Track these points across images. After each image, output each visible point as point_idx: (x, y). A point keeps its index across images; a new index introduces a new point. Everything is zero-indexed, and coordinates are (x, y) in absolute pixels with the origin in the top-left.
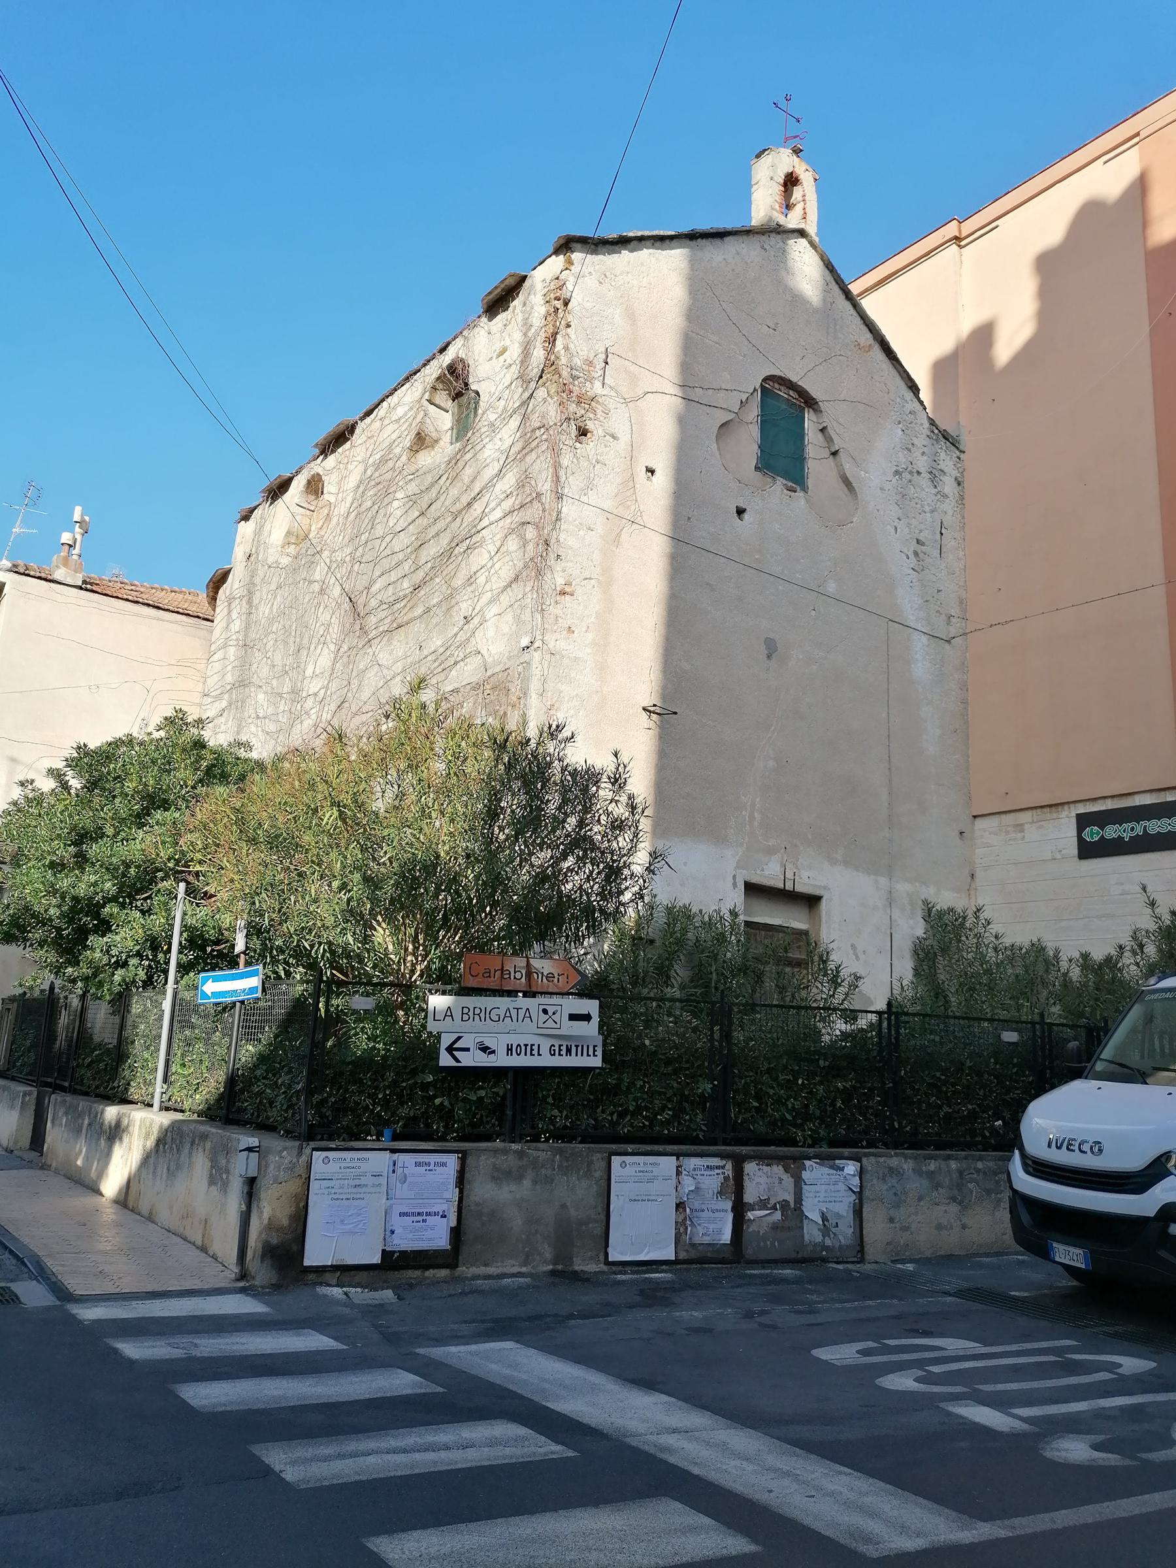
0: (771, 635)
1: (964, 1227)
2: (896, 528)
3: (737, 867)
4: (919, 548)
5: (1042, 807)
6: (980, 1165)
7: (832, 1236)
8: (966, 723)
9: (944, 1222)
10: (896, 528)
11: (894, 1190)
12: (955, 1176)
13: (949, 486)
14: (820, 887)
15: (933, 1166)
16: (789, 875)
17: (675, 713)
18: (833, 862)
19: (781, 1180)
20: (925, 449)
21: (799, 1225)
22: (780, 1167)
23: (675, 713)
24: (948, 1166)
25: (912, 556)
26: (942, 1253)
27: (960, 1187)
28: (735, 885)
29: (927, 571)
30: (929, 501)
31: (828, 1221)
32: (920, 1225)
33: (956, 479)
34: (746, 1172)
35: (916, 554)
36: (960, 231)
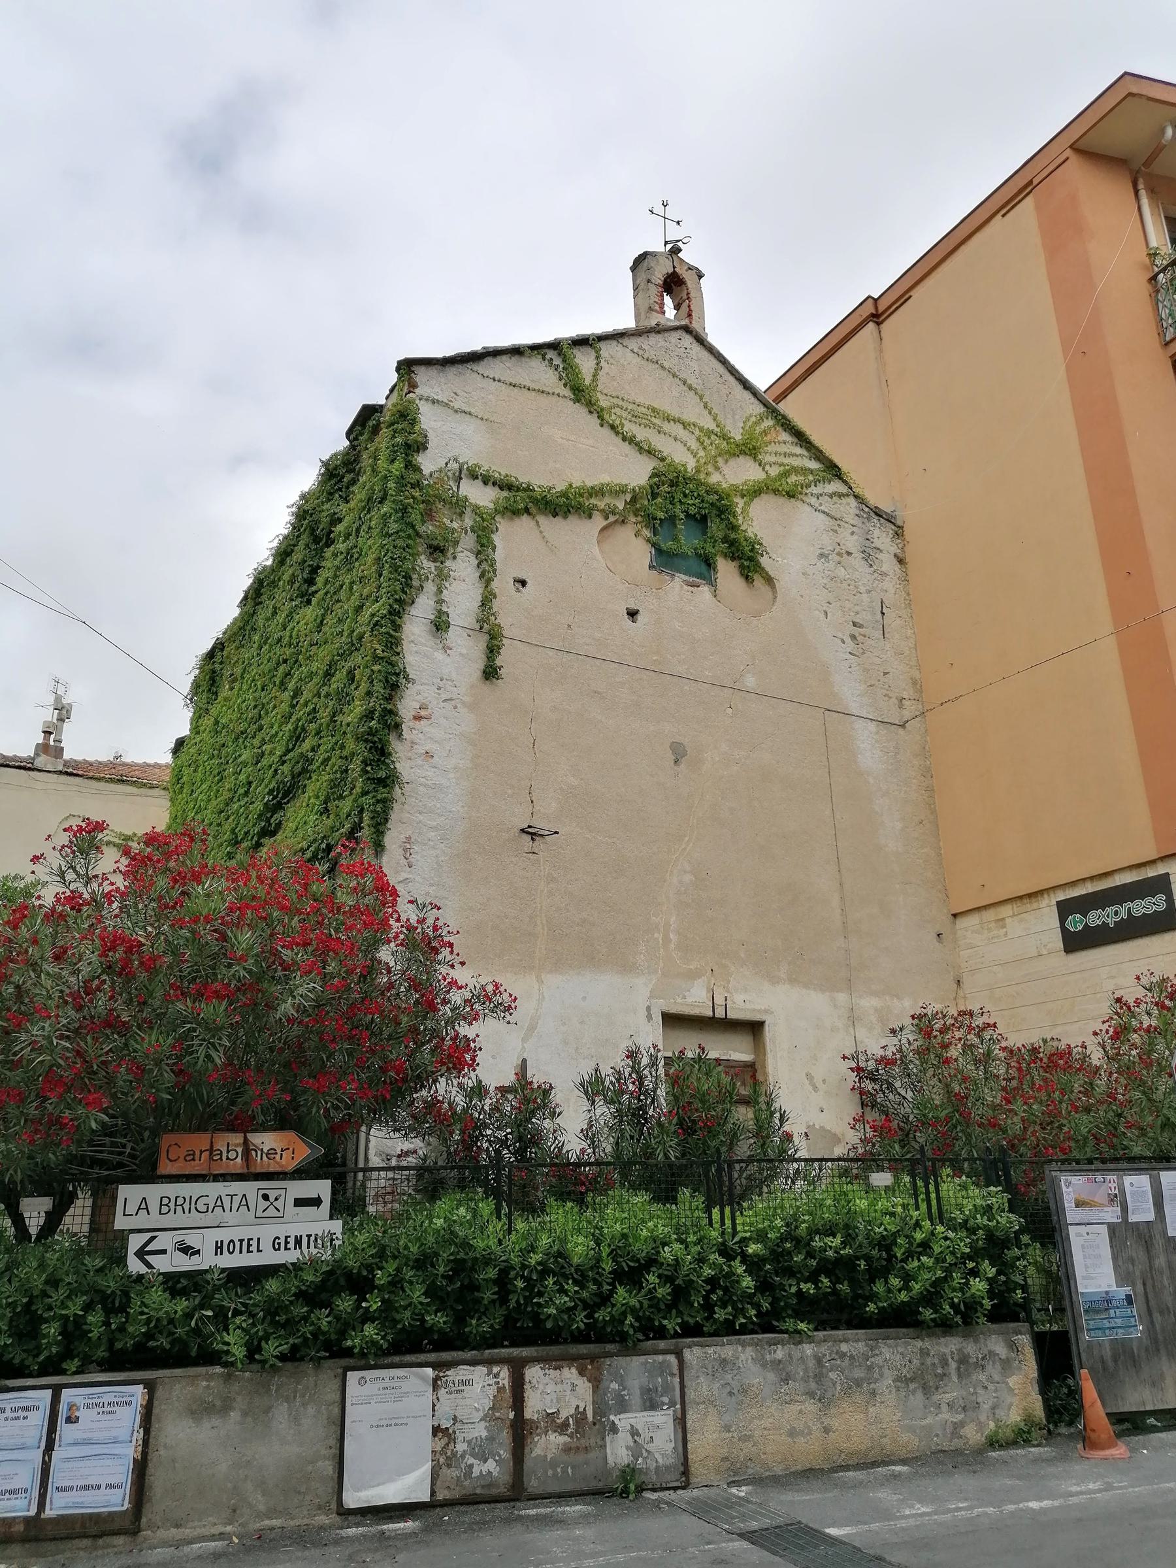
0: (678, 739)
1: (827, 1430)
2: (826, 613)
3: (651, 997)
4: (856, 631)
5: (1021, 897)
6: (844, 1347)
7: (645, 1454)
8: (934, 812)
9: (799, 1425)
10: (826, 613)
11: (728, 1389)
12: (811, 1363)
13: (887, 563)
14: (759, 1011)
15: (780, 1353)
16: (719, 1000)
17: (557, 833)
18: (774, 980)
19: (574, 1386)
20: (855, 529)
21: (600, 1443)
22: (574, 1370)
23: (557, 833)
24: (803, 1352)
25: (848, 640)
26: (799, 1467)
27: (819, 1378)
28: (649, 1017)
29: (868, 654)
30: (865, 581)
31: (639, 1435)
32: (766, 1432)
33: (895, 555)
34: (527, 1380)
35: (853, 637)
36: (876, 308)
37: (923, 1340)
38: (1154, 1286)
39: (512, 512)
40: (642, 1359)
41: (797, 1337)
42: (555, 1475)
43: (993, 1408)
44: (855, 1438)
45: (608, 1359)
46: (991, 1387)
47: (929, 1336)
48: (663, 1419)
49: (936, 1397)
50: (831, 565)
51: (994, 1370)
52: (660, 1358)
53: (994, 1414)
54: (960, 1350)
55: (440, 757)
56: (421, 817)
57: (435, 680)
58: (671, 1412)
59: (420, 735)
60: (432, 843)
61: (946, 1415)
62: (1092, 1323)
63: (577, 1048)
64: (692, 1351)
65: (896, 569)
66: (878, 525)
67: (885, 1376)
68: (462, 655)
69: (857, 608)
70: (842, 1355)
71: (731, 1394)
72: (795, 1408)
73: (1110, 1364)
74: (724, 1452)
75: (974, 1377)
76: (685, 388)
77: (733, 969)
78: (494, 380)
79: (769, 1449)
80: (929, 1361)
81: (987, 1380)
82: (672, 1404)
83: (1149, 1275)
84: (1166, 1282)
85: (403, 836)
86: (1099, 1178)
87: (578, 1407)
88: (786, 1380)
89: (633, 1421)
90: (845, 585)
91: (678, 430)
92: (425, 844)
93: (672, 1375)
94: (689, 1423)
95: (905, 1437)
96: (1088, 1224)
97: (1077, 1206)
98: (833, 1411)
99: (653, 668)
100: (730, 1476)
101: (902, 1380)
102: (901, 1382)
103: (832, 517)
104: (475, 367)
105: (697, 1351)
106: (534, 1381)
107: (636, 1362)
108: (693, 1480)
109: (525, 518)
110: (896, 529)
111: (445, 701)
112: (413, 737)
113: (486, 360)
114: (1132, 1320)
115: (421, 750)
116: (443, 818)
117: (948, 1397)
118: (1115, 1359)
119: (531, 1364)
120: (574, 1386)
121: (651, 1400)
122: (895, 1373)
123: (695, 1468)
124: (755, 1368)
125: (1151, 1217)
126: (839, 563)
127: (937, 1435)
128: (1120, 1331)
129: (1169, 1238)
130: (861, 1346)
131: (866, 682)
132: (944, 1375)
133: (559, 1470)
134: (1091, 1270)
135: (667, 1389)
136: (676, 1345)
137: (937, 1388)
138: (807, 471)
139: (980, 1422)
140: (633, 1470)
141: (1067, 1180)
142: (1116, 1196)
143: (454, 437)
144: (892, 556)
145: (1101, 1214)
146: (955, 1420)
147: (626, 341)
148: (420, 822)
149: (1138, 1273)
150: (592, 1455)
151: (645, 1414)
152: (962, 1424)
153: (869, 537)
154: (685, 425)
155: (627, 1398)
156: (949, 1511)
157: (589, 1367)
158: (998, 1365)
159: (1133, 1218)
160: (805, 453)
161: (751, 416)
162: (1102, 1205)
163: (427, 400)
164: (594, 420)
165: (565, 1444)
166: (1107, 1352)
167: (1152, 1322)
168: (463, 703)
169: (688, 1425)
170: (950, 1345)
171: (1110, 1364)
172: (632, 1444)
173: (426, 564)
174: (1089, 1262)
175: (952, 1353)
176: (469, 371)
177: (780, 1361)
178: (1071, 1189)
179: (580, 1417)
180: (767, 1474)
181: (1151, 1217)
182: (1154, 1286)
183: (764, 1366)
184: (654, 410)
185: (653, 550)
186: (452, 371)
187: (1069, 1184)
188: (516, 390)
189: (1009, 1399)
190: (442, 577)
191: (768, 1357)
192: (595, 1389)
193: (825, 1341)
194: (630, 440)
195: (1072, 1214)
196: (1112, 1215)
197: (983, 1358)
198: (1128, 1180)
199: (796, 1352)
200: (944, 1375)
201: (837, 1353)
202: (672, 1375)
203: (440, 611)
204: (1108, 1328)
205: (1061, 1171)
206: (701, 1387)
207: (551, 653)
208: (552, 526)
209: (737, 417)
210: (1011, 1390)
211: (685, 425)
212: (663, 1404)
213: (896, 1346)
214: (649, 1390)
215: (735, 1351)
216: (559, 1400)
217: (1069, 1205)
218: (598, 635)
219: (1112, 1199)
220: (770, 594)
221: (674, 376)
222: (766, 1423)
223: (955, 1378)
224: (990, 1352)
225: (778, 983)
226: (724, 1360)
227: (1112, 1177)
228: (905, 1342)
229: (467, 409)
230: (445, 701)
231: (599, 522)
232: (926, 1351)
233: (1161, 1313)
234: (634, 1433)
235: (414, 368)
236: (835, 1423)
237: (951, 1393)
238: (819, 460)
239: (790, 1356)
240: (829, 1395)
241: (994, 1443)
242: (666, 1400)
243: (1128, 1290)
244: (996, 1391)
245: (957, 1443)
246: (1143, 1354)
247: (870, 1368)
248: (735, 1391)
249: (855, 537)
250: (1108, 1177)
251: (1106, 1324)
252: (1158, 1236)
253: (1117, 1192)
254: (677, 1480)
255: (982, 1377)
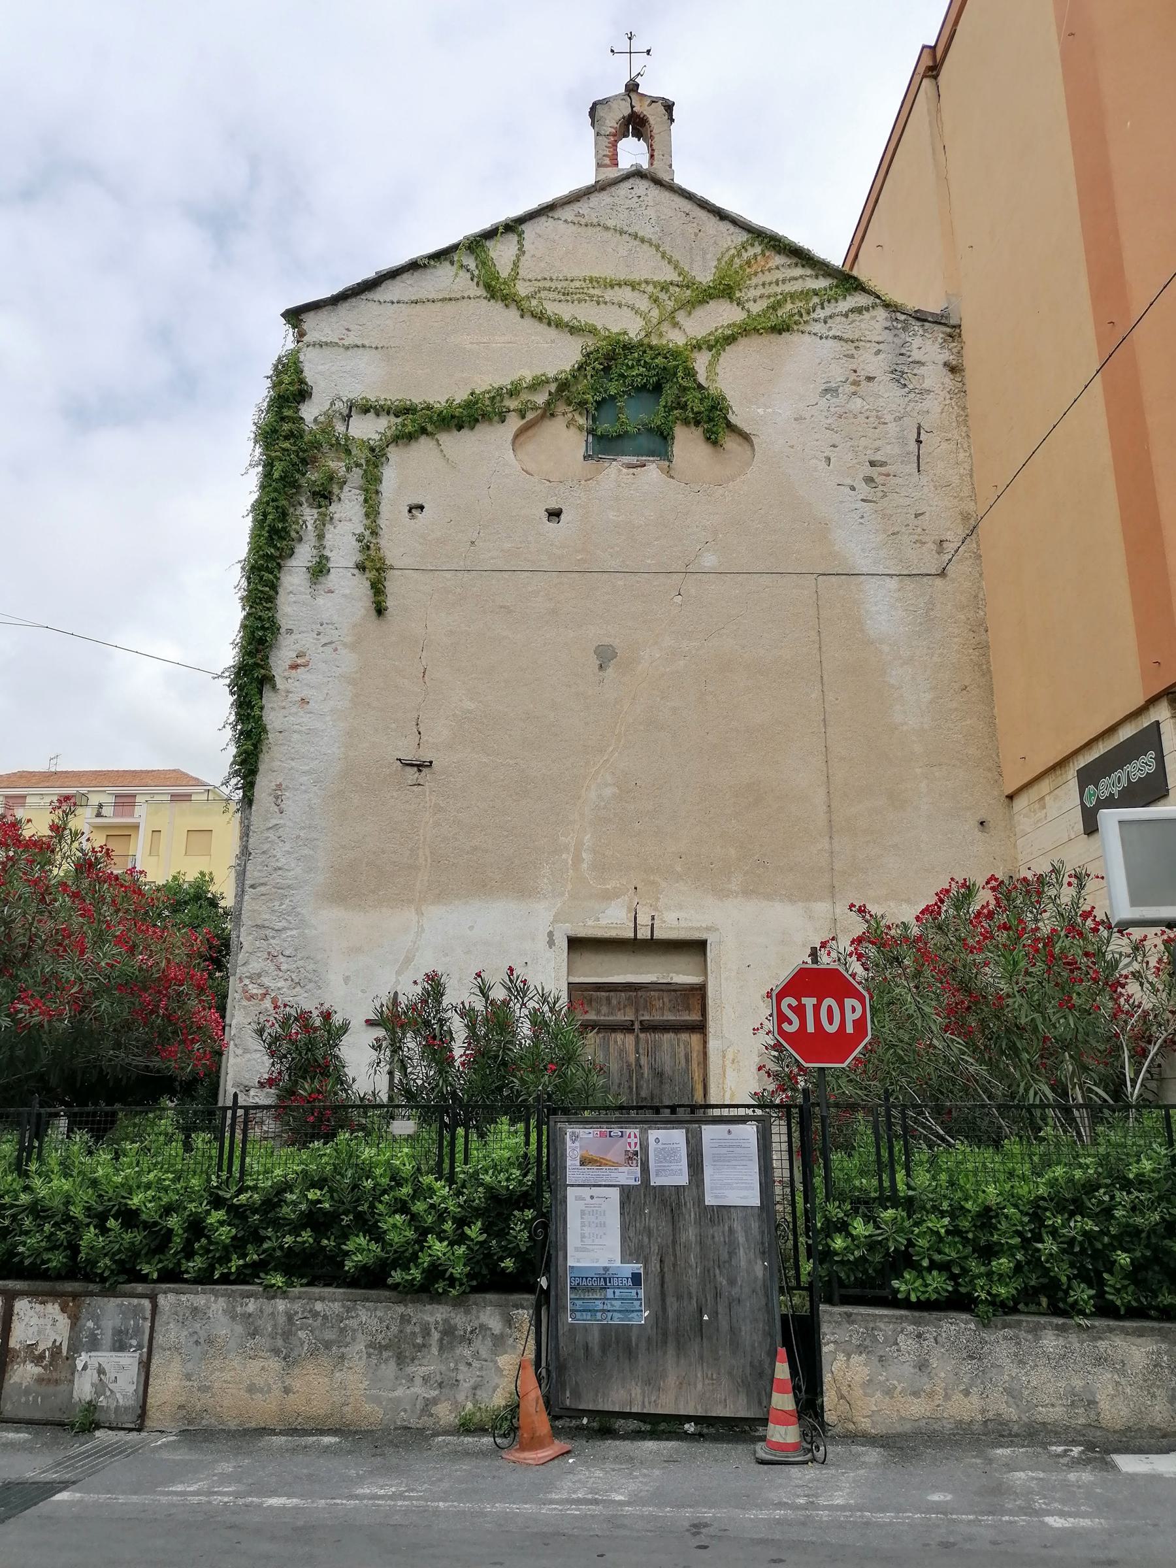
0: (606, 641)
1: (287, 1390)
2: (828, 459)
3: (556, 920)
4: (874, 472)
6: (319, 1306)
7: (108, 1393)
8: (987, 673)
9: (259, 1381)
10: (828, 459)
11: (195, 1337)
12: (282, 1320)
13: (933, 377)
14: (698, 929)
15: (252, 1306)
16: (644, 919)
18: (721, 894)
19: (55, 1321)
20: (881, 347)
21: (69, 1378)
22: (57, 1306)
24: (275, 1307)
26: (253, 1425)
27: (287, 1335)
28: (551, 943)
29: (890, 496)
30: (894, 407)
31: (104, 1373)
32: (225, 1385)
33: (945, 364)
34: (16, 1312)
37: (406, 1306)
38: (674, 1265)
39: (404, 438)
40: (119, 1300)
41: (271, 1292)
42: (27, 1401)
43: (475, 1388)
44: (315, 1403)
45: (88, 1298)
46: (476, 1364)
47: (413, 1302)
48: (129, 1360)
49: (411, 1369)
50: (842, 398)
51: (483, 1347)
52: (135, 1301)
53: (474, 1394)
54: (446, 1321)
55: (316, 702)
56: (293, 764)
57: (314, 627)
58: (137, 1355)
59: (297, 683)
60: (303, 787)
61: (418, 1389)
62: (579, 1303)
63: (460, 979)
64: (166, 1297)
65: (947, 380)
66: (921, 332)
67: (358, 1340)
68: (344, 596)
69: (878, 443)
70: (315, 1314)
71: (197, 1343)
72: (257, 1364)
73: (596, 1349)
74: (182, 1400)
75: (458, 1352)
76: (637, 243)
77: (664, 884)
78: (393, 303)
79: (225, 1403)
80: (409, 1329)
81: (473, 1356)
82: (139, 1347)
83: (671, 1250)
84: (693, 1260)
85: (273, 784)
86: (616, 1131)
87: (55, 1340)
88: (253, 1335)
89: (101, 1360)
90: (861, 419)
91: (626, 294)
92: (297, 790)
93: (145, 1319)
94: (153, 1368)
95: (368, 1408)
96: (594, 1186)
97: (582, 1164)
98: (297, 1371)
99: (576, 568)
100: (184, 1424)
101: (376, 1347)
102: (375, 1348)
103: (846, 341)
104: (370, 295)
105: (171, 1297)
106: (22, 1314)
107: (112, 1303)
108: (148, 1423)
109: (423, 439)
110: (948, 330)
111: (325, 645)
112: (288, 686)
113: (383, 285)
114: (637, 1303)
115: (295, 697)
116: (318, 761)
117: (423, 1371)
118: (604, 1348)
119: (21, 1297)
120: (55, 1321)
121: (120, 1341)
122: (370, 1338)
123: (152, 1413)
124: (224, 1320)
125: (683, 1180)
126: (854, 393)
127: (405, 1410)
128: (616, 1315)
129: (706, 1207)
130: (337, 1307)
131: (885, 531)
132: (424, 1345)
133: (31, 1399)
134: (588, 1241)
135: (138, 1331)
136: (153, 1290)
137: (413, 1360)
138: (806, 295)
139: (456, 1402)
140: (95, 1407)
141: (573, 1133)
142: (636, 1153)
143: (345, 374)
144: (941, 366)
145: (613, 1175)
146: (427, 1396)
147: (559, 213)
148: (292, 768)
149: (655, 1248)
150: (62, 1387)
151: (113, 1354)
152: (435, 1401)
153: (903, 351)
154: (633, 286)
155: (99, 1337)
156: (357, 1497)
157: (71, 1304)
158: (489, 1342)
159: (656, 1181)
160: (809, 272)
161: (728, 249)
162: (616, 1164)
163: (314, 345)
164: (513, 313)
165: (39, 1375)
166: (595, 1339)
167: (664, 1309)
168: (345, 645)
169: (152, 1369)
170: (435, 1314)
171: (596, 1349)
172: (97, 1382)
173: (308, 514)
174: (587, 1230)
175: (437, 1322)
176: (364, 302)
177: (250, 1315)
178: (577, 1144)
179: (56, 1350)
180: (221, 1427)
181: (683, 1180)
182: (674, 1265)
183: (233, 1318)
184: (591, 280)
185: (590, 438)
186: (343, 308)
187: (575, 1138)
188: (418, 306)
189: (497, 1380)
190: (324, 520)
191: (239, 1309)
192: (73, 1326)
193: (299, 1298)
194: (558, 324)
195: (573, 1171)
196: (628, 1176)
197: (471, 1332)
198: (653, 1134)
199: (268, 1307)
200: (424, 1345)
201: (311, 1311)
202: (145, 1319)
203: (322, 557)
204: (600, 1311)
205: (570, 1122)
206: (170, 1333)
207: (448, 575)
208: (456, 443)
209: (709, 256)
210: (499, 1370)
211: (633, 286)
212: (131, 1346)
213: (375, 1309)
214: (120, 1332)
215: (208, 1300)
216: (39, 1332)
217: (572, 1162)
218: (507, 545)
219: (630, 1158)
220: (749, 453)
221: (622, 232)
222: (227, 1376)
223: (435, 1350)
224: (482, 1326)
225: (728, 896)
226: (196, 1308)
227: (633, 1132)
228: (385, 1307)
229: (359, 343)
230: (325, 645)
231: (514, 423)
232: (407, 1317)
233: (679, 1298)
234: (101, 1371)
235: (303, 317)
236: (296, 1384)
237: (430, 1365)
238: (830, 275)
239: (261, 1311)
240: (294, 1354)
241: (467, 1427)
242: (134, 1342)
243: (638, 1267)
244: (481, 1369)
245: (426, 1421)
246: (643, 1345)
247: (342, 1331)
248: (202, 1341)
249: (882, 356)
250: (628, 1131)
251: (599, 1305)
252: (690, 1205)
253: (638, 1148)
254: (133, 1422)
255: (467, 1352)
